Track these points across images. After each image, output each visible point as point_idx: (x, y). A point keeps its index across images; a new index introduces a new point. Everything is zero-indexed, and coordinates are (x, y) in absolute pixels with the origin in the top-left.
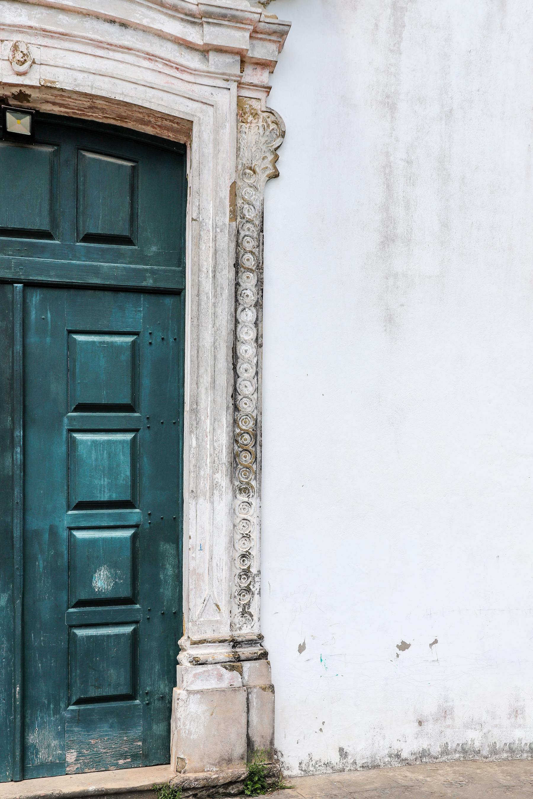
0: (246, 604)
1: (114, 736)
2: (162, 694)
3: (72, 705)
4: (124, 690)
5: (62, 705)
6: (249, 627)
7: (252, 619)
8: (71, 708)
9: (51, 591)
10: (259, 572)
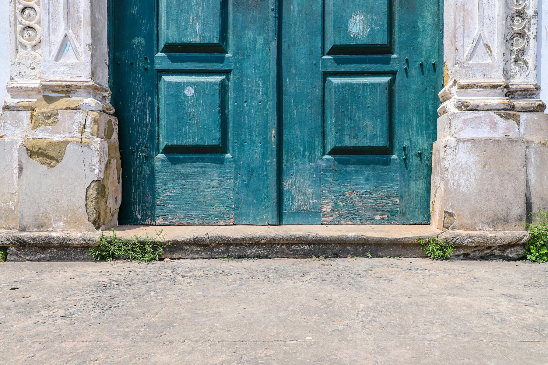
0: (520, 50)
1: (371, 190)
2: (420, 150)
3: (327, 155)
4: (381, 142)
5: (318, 153)
6: (524, 75)
7: (528, 67)
8: (326, 157)
9: (306, 36)
10: (536, 13)
